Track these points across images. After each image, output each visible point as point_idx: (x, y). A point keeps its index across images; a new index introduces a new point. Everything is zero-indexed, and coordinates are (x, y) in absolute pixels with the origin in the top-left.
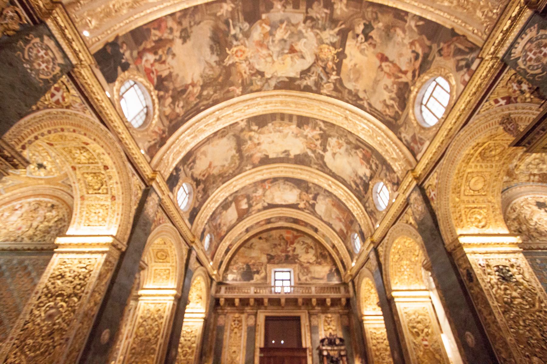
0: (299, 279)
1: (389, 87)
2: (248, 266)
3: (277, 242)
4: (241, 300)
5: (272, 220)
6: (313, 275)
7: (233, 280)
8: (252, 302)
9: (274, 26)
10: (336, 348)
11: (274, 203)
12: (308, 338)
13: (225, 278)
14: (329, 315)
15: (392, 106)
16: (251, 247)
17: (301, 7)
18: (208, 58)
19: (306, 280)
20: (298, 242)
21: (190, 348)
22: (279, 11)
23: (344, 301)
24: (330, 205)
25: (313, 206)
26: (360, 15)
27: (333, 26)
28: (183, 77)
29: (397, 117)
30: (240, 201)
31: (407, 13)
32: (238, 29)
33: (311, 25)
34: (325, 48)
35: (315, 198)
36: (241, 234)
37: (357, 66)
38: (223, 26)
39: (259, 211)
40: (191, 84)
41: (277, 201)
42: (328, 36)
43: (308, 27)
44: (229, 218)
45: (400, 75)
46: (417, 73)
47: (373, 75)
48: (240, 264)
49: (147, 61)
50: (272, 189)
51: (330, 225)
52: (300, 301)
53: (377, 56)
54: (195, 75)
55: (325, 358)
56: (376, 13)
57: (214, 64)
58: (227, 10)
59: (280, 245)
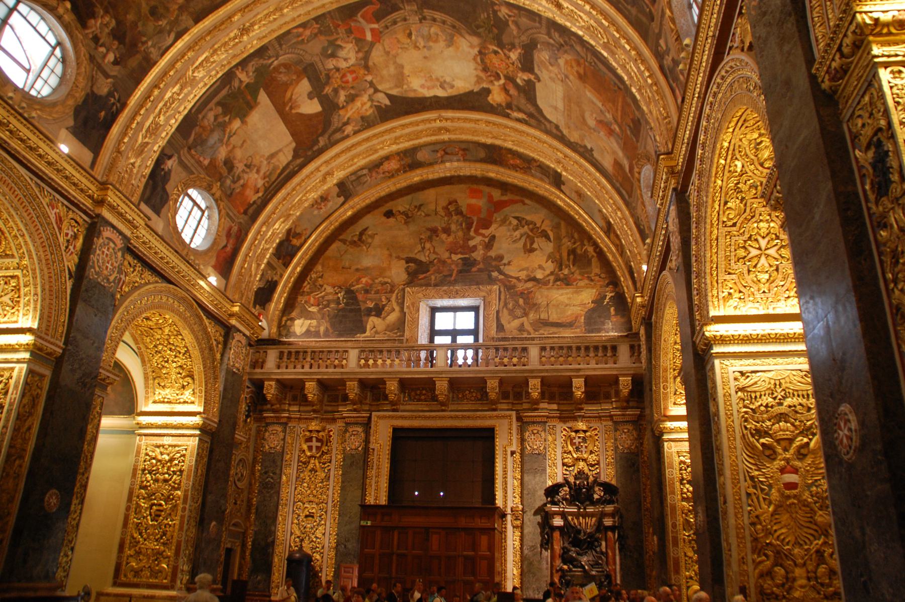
0: (500, 327)
2: (350, 294)
3: (439, 224)
4: (323, 385)
5: (421, 156)
6: (543, 316)
7: (308, 333)
8: (353, 390)
10: (590, 509)
11: (412, 95)
12: (513, 483)
13: (283, 327)
14: (581, 425)
16: (360, 241)
19: (521, 328)
20: (504, 221)
21: (167, 499)
23: (625, 383)
24: (573, 79)
25: (529, 91)
30: (286, 86)
35: (527, 64)
36: (324, 199)
39: (367, 123)
41: (418, 87)
44: (265, 148)
48: (329, 289)
50: (387, 42)
51: (586, 154)
52: (492, 385)
55: (557, 534)
59: (447, 231)
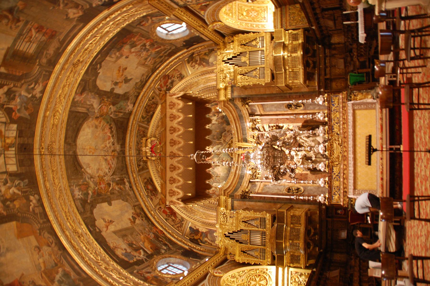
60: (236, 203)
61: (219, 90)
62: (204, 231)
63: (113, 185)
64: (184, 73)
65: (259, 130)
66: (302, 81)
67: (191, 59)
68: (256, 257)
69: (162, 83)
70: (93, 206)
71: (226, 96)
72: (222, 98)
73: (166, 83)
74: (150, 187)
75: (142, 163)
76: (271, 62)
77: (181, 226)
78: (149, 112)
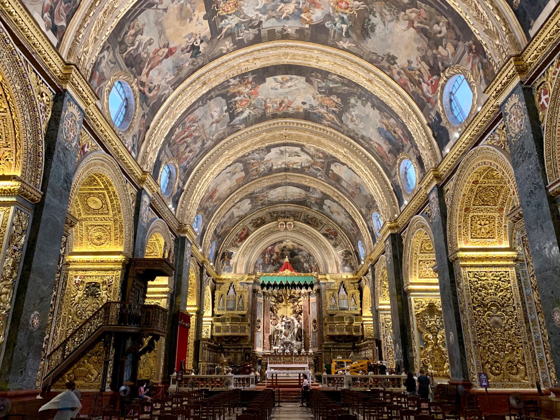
1: (148, 47)
9: (296, 15)
15: (133, 44)
17: (266, 32)
18: (382, 26)
22: (289, 27)
26: (206, 54)
27: (229, 31)
28: (415, 40)
29: (123, 47)
31: (174, 89)
32: (337, 25)
33: (253, 22)
34: (232, 10)
37: (188, 20)
38: (353, 36)
40: (413, 27)
42: (230, 22)
43: (256, 20)
45: (150, 66)
46: (142, 88)
47: (169, 32)
49: (428, 91)
53: (175, 48)
54: (403, 28)
56: (195, 66)
57: (377, 15)
58: (345, 42)
60: (251, 286)
61: (325, 274)
62: (231, 263)
63: (262, 202)
64: (338, 247)
65: (299, 298)
66: (329, 333)
67: (348, 253)
68: (219, 304)
69: (332, 231)
70: (249, 198)
71: (321, 279)
72: (320, 277)
73: (331, 233)
74: (259, 222)
75: (275, 215)
76: (340, 315)
77: (233, 246)
78: (311, 221)
